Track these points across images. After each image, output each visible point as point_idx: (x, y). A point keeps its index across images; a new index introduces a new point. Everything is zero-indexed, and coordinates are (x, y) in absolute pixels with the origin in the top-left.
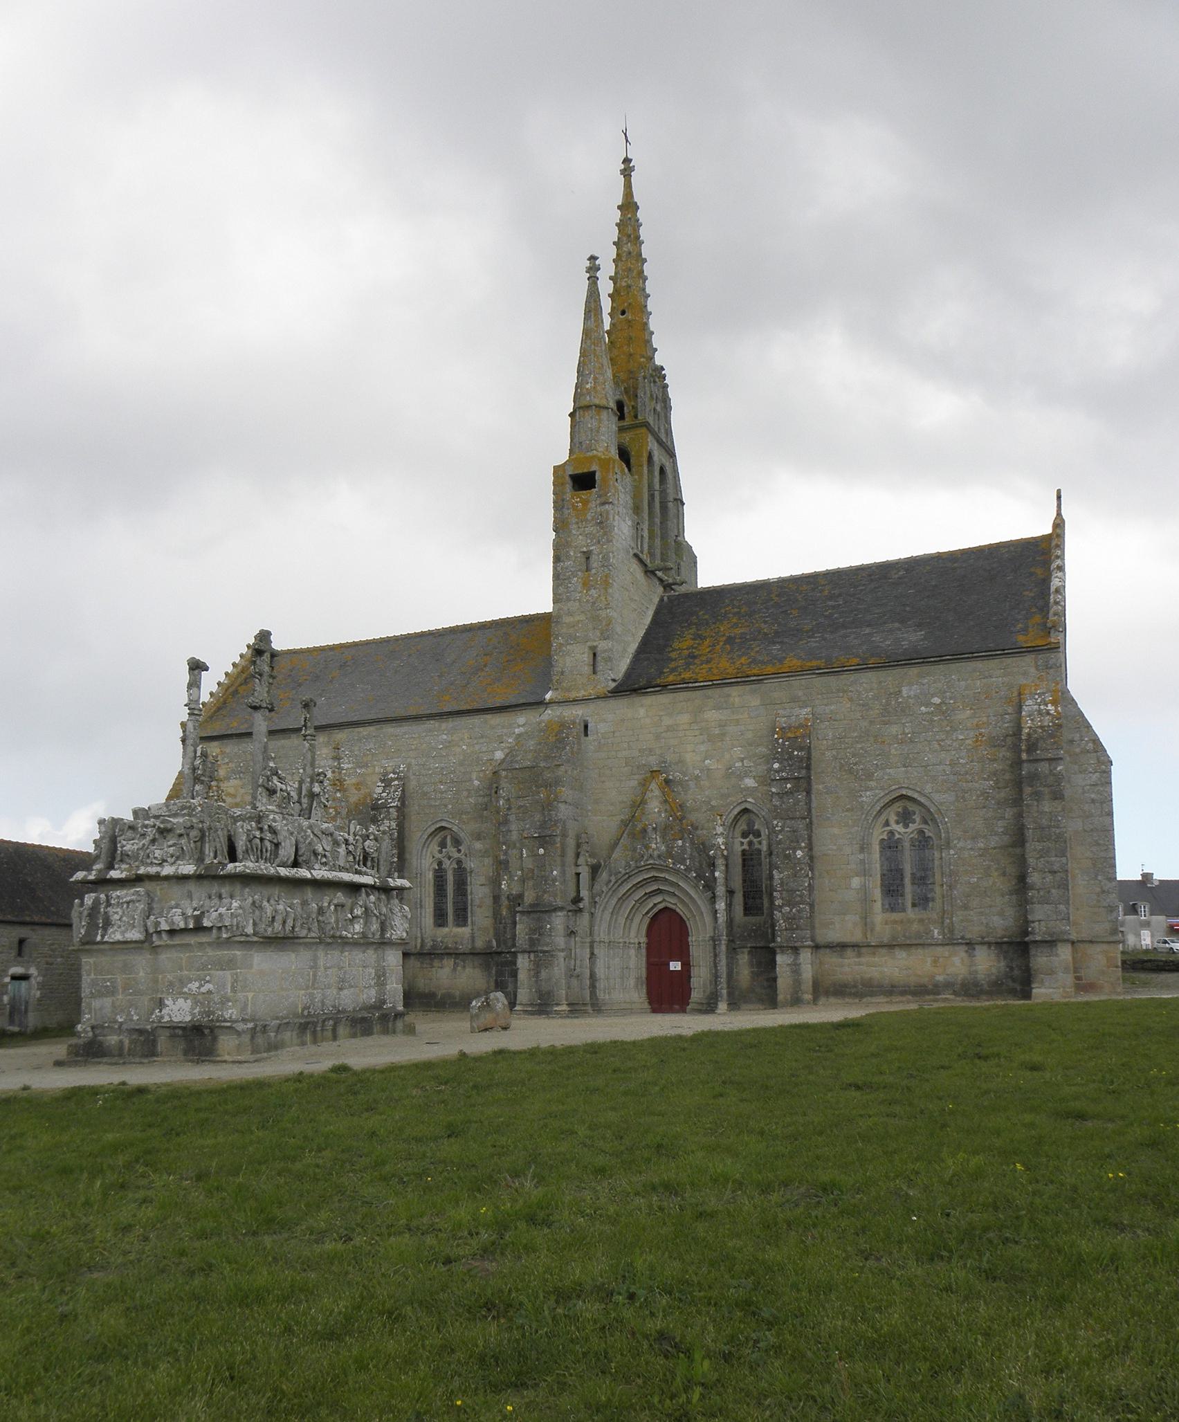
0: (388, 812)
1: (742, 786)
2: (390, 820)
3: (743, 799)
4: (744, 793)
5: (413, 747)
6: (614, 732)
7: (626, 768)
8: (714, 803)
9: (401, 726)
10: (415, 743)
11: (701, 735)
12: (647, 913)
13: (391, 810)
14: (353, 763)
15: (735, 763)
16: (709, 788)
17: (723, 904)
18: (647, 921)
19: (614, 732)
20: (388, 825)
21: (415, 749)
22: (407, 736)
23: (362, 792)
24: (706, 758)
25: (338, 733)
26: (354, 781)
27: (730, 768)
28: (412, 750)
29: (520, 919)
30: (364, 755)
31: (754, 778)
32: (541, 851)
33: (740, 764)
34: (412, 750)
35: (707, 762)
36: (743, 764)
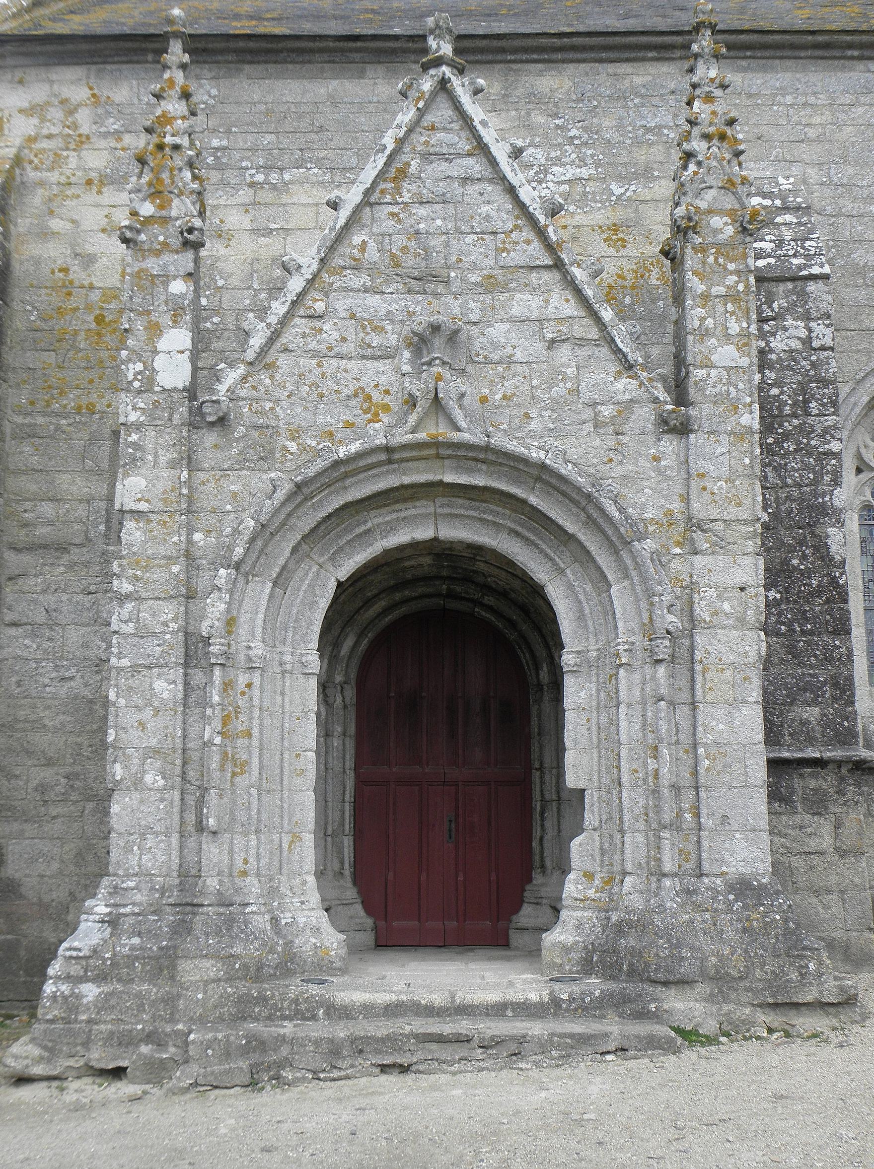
0: (804, 296)
2: (807, 317)
5: (812, 133)
9: (764, 69)
10: (817, 120)
13: (811, 287)
14: (598, 165)
20: (803, 333)
21: (818, 140)
22: (789, 99)
23: (632, 251)
25: (540, 74)
26: (600, 217)
28: (811, 141)
30: (638, 143)
34: (811, 141)
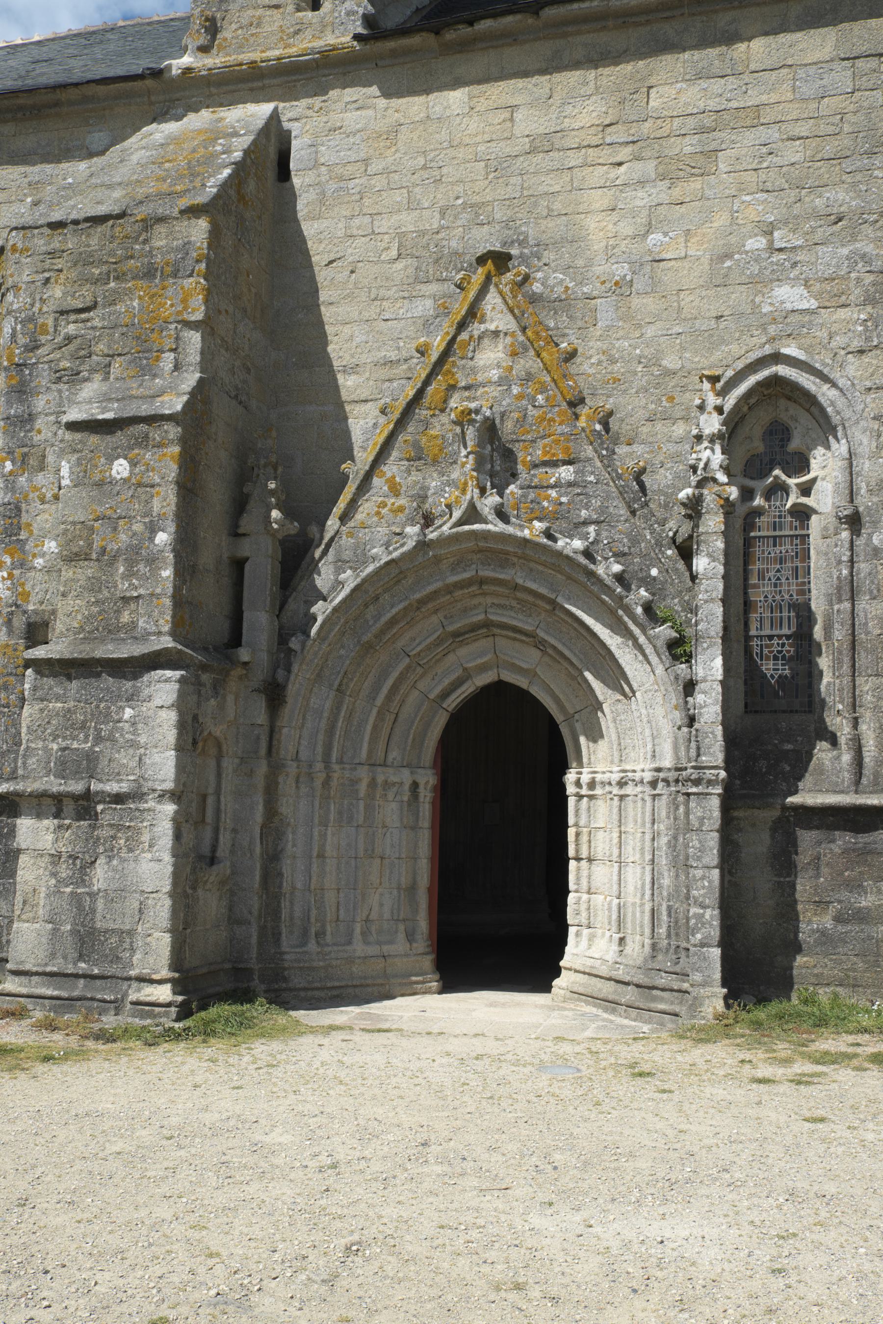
1: (766, 309)
3: (768, 350)
4: (772, 330)
6: (366, 161)
7: (399, 265)
8: (670, 362)
11: (638, 158)
12: (445, 695)
15: (744, 238)
16: (658, 318)
17: (719, 662)
18: (441, 721)
19: (366, 161)
24: (649, 228)
27: (728, 256)
29: (35, 689)
31: (806, 284)
32: (121, 468)
33: (757, 243)
35: (654, 238)
36: (771, 242)
